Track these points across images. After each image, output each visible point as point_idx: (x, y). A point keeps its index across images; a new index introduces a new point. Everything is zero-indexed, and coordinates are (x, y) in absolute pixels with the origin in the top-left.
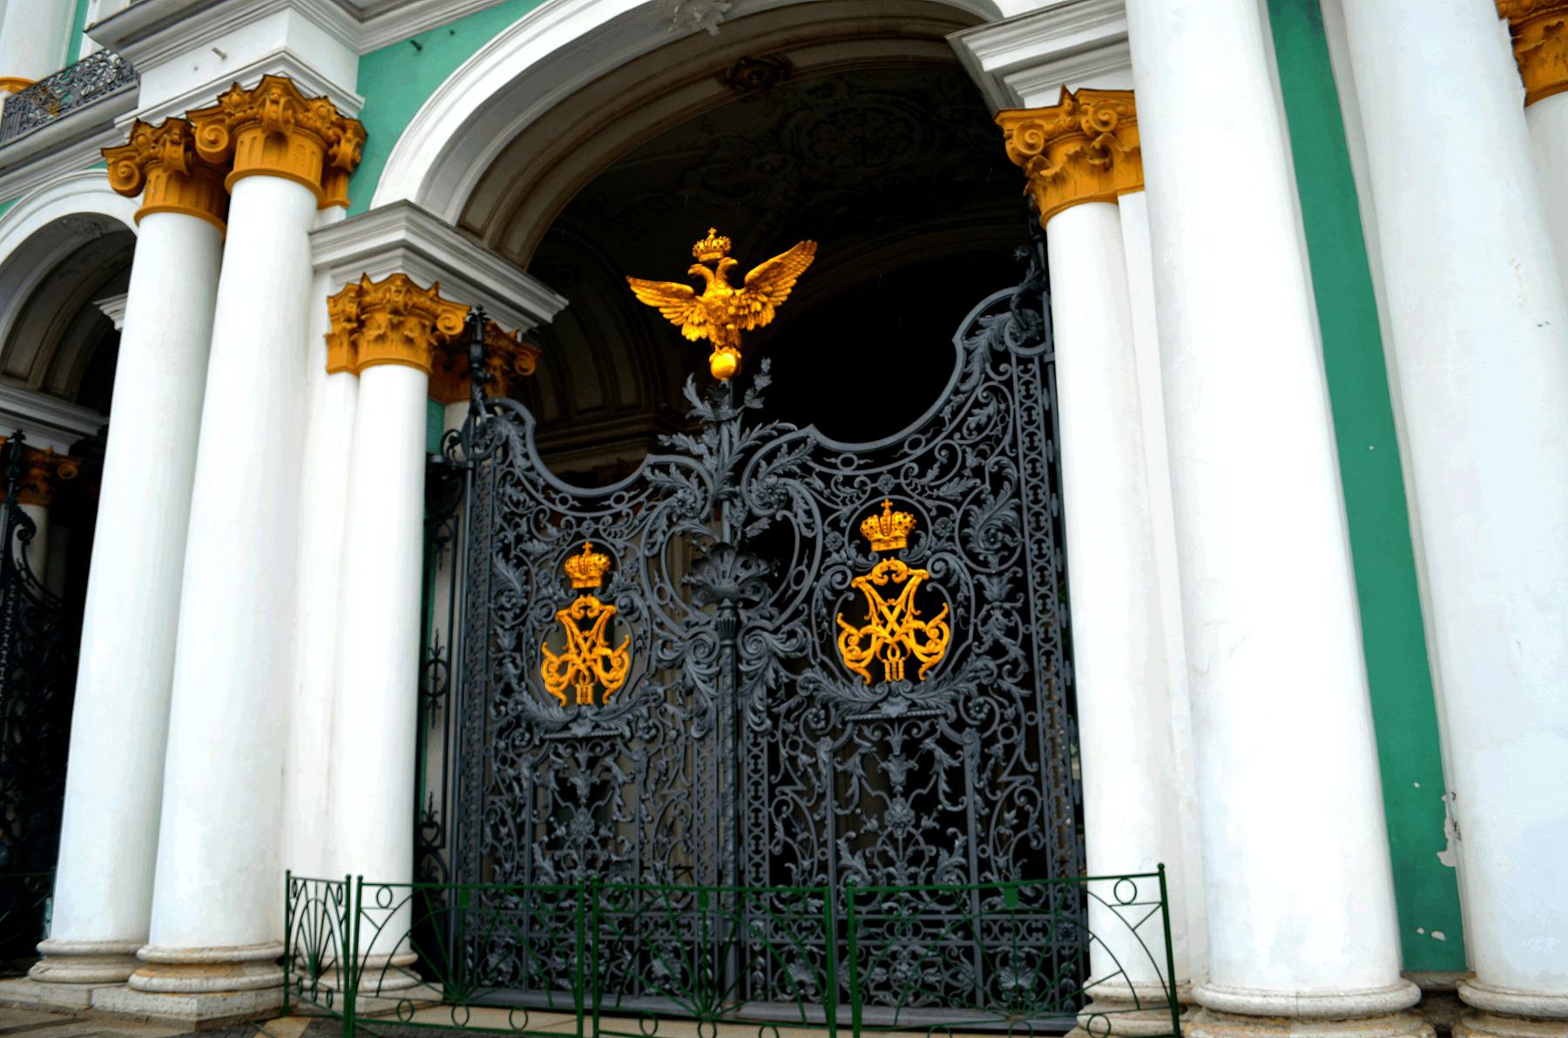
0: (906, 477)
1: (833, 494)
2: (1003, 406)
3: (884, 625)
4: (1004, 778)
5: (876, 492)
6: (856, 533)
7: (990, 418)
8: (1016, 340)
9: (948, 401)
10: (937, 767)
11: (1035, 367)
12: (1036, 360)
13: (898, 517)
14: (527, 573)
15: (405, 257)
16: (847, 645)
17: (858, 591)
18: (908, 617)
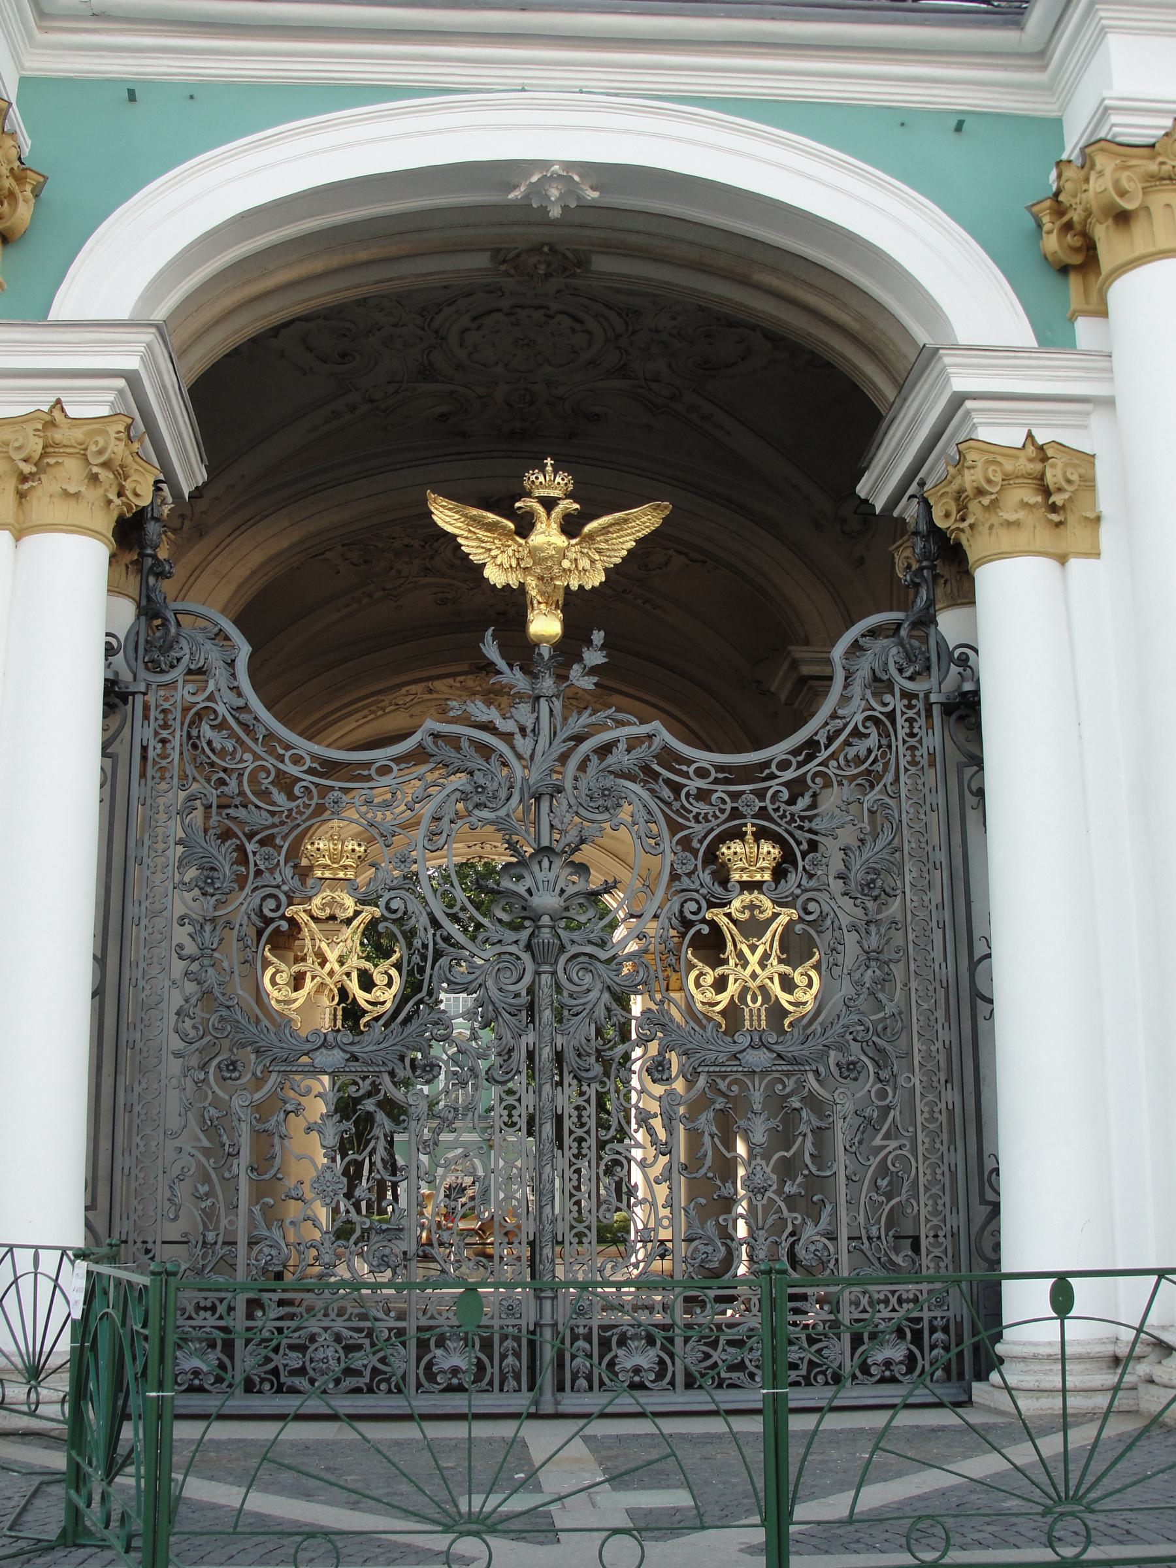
0: (773, 802)
1: (683, 807)
2: (884, 742)
3: (744, 967)
4: (878, 1142)
5: (736, 813)
6: (711, 856)
7: (870, 751)
8: (901, 671)
9: (826, 724)
10: (803, 1128)
11: (920, 705)
12: (921, 695)
13: (766, 847)
14: (241, 849)
15: (120, 392)
16: (698, 985)
17: (713, 924)
18: (774, 960)
